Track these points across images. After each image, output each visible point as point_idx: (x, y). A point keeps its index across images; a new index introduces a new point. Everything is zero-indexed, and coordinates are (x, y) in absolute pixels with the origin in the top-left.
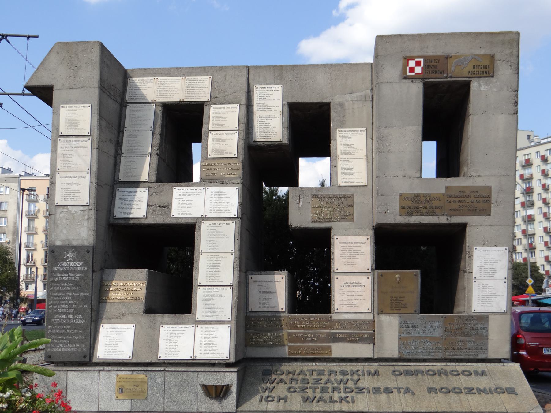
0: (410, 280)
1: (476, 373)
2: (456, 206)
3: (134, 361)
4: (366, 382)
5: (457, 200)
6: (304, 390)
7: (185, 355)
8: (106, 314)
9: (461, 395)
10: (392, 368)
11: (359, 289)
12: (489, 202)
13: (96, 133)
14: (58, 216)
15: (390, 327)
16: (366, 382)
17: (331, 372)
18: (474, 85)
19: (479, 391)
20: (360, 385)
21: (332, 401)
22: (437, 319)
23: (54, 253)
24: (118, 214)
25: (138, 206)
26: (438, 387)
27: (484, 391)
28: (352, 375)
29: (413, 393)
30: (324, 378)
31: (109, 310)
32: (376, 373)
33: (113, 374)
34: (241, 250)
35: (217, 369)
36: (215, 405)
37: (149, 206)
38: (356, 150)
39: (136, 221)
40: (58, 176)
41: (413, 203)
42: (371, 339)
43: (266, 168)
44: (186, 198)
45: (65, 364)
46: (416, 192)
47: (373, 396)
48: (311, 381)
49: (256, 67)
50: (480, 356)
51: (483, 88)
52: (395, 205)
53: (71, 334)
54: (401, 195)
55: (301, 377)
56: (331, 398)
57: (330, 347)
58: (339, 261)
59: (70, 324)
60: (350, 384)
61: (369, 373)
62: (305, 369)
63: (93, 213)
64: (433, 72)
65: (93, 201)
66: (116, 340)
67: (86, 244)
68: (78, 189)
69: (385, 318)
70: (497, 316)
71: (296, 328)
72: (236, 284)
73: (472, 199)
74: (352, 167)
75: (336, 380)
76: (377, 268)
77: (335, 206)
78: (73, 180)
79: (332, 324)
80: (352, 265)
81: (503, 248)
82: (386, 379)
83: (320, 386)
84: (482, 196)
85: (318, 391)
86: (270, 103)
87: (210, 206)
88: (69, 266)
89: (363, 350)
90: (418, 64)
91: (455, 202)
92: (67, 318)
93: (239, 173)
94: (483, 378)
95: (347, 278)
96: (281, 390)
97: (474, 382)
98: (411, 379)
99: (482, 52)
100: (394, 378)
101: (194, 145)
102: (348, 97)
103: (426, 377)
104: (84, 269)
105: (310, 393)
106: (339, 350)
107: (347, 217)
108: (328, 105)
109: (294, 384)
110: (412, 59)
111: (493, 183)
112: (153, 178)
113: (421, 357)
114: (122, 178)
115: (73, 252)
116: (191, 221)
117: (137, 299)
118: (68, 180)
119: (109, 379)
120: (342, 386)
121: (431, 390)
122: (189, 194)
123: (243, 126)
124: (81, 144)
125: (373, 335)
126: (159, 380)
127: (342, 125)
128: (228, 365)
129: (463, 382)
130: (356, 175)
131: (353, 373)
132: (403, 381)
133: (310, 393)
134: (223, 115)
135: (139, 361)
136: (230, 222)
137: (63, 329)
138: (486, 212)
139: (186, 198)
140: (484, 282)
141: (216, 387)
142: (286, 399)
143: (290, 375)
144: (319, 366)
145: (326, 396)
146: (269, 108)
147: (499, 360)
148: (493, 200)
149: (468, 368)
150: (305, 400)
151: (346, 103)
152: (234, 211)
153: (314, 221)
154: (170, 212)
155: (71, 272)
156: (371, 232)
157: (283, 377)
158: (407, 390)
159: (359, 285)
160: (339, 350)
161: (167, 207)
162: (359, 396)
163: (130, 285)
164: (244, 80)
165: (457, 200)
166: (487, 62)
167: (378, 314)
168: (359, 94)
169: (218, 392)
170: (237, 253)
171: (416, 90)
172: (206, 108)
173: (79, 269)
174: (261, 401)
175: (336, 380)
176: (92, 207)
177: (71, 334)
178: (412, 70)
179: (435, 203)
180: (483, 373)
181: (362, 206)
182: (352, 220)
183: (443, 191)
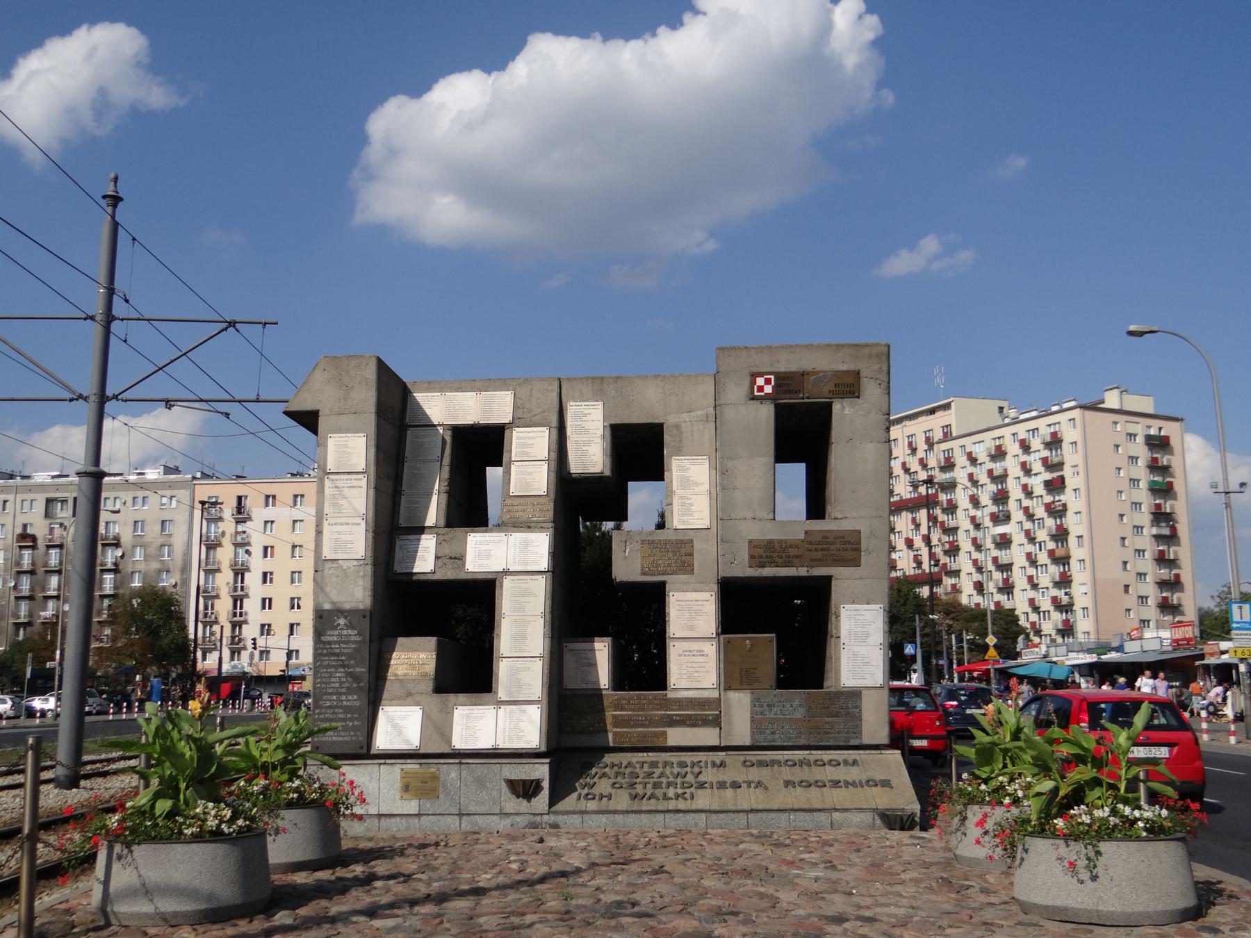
0: (763, 647)
1: (846, 763)
2: (818, 555)
3: (422, 751)
4: (709, 775)
5: (819, 547)
6: (632, 785)
7: (485, 743)
8: (386, 695)
9: (824, 789)
10: (742, 758)
11: (701, 659)
12: (858, 550)
13: (372, 468)
14: (326, 572)
15: (740, 705)
16: (709, 775)
17: (666, 764)
18: (836, 407)
19: (847, 784)
20: (702, 778)
21: (666, 798)
22: (797, 696)
23: (323, 620)
24: (398, 568)
25: (425, 559)
26: (797, 780)
27: (854, 784)
28: (693, 767)
29: (766, 788)
30: (658, 772)
31: (390, 689)
32: (723, 764)
33: (397, 769)
34: (552, 612)
35: (525, 761)
36: (523, 805)
37: (437, 558)
38: (696, 484)
39: (422, 577)
40: (325, 523)
41: (765, 552)
42: (716, 722)
43: (584, 507)
44: (484, 547)
45: (337, 757)
46: (768, 538)
47: (716, 791)
48: (641, 775)
49: (569, 380)
50: (853, 742)
51: (847, 411)
52: (744, 555)
53: (344, 720)
54: (750, 542)
55: (628, 770)
56: (665, 794)
57: (665, 733)
58: (676, 624)
59: (341, 707)
60: (690, 778)
61: (714, 764)
62: (634, 760)
63: (369, 569)
64: (786, 392)
65: (369, 554)
66: (399, 726)
67: (361, 607)
68: (351, 538)
69: (734, 696)
70: (873, 691)
71: (622, 710)
72: (547, 654)
73: (838, 546)
74: (692, 505)
75: (672, 773)
76: (724, 632)
77: (671, 555)
78: (344, 528)
79: (667, 703)
80: (692, 628)
81: (877, 607)
82: (735, 769)
83: (651, 781)
84: (849, 543)
85: (649, 786)
86: (587, 425)
87: (514, 557)
88: (340, 635)
89: (707, 736)
90: (768, 382)
91: (816, 550)
92: (339, 700)
93: (550, 515)
94: (854, 768)
96: (603, 786)
97: (841, 773)
98: (764, 770)
99: (845, 367)
100: (744, 769)
101: (490, 471)
102: (685, 417)
103: (783, 769)
104: (358, 638)
105: (639, 789)
106: (676, 736)
107: (686, 567)
108: (661, 426)
109: (619, 779)
110: (761, 375)
111: (862, 526)
112: (442, 522)
113: (779, 743)
114: (403, 522)
115: (346, 618)
116: (490, 577)
117: (425, 675)
118: (338, 528)
119: (392, 774)
120: (679, 780)
121: (787, 783)
122: (488, 543)
123: (554, 455)
124: (355, 483)
125: (718, 717)
126: (453, 775)
127: (679, 452)
128: (536, 755)
129: (829, 773)
130: (696, 515)
131: (693, 765)
132: (754, 774)
133: (639, 789)
134: (529, 442)
135: (429, 751)
136: (539, 577)
137: (334, 713)
138: (855, 562)
139: (484, 547)
140: (856, 649)
141: (524, 782)
142: (610, 797)
143: (616, 769)
144: (652, 756)
145: (659, 793)
146: (587, 432)
147: (877, 747)
148: (863, 548)
149: (836, 757)
150: (634, 797)
151: (684, 425)
153: (644, 574)
154: (464, 565)
155: (344, 642)
156: (715, 587)
157: (607, 770)
158: (759, 784)
159: (701, 653)
160: (676, 736)
161: (460, 558)
162: (700, 792)
163: (414, 658)
164: (555, 395)
165: (819, 547)
166: (850, 380)
167: (725, 690)
168: (699, 413)
169: (526, 789)
170: (548, 616)
171: (766, 413)
172: (507, 432)
173: (353, 638)
174: (579, 799)
175: (672, 773)
176: (369, 561)
177: (344, 720)
178: (761, 389)
179: (793, 552)
180: (855, 763)
181: (705, 553)
182: (692, 572)
183: (802, 536)
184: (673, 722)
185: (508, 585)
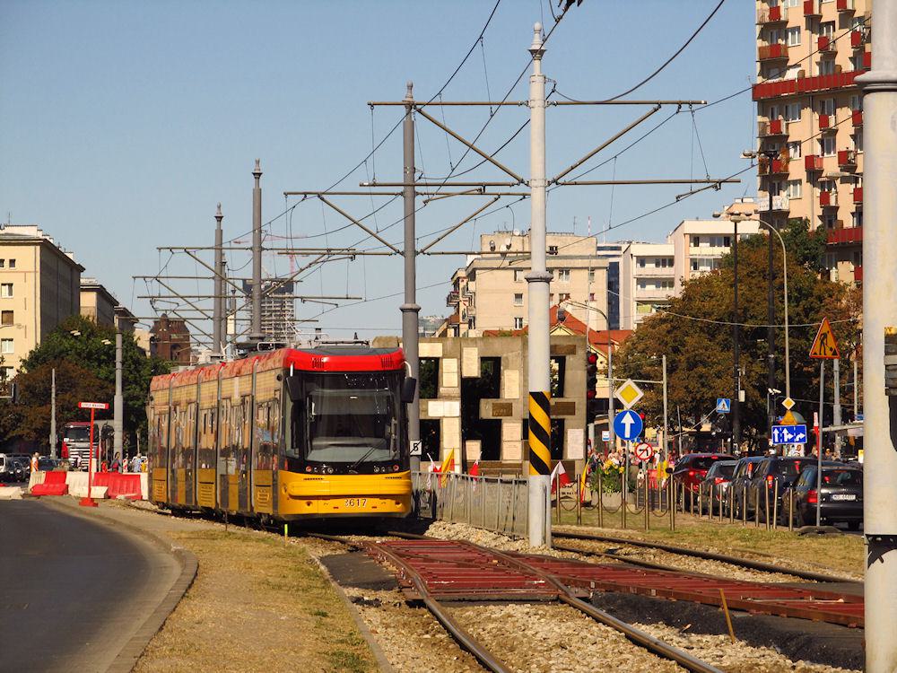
18: (567, 358)
51: (571, 359)
79: (502, 465)
93: (460, 395)
95: (509, 443)
102: (510, 354)
108: (500, 358)
111: (576, 401)
127: (507, 368)
152: (458, 413)
172: (440, 361)
184: (504, 473)
185: (445, 420)
